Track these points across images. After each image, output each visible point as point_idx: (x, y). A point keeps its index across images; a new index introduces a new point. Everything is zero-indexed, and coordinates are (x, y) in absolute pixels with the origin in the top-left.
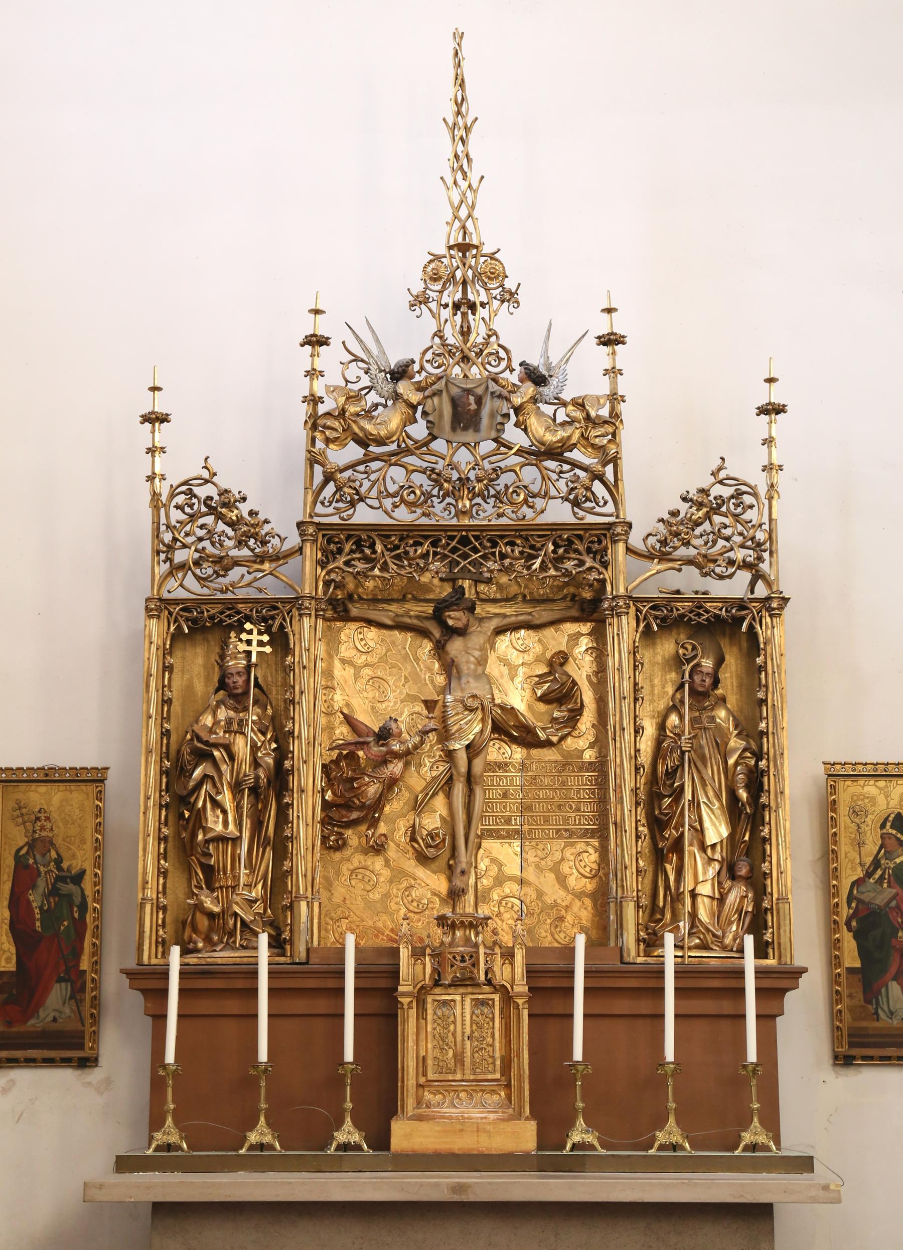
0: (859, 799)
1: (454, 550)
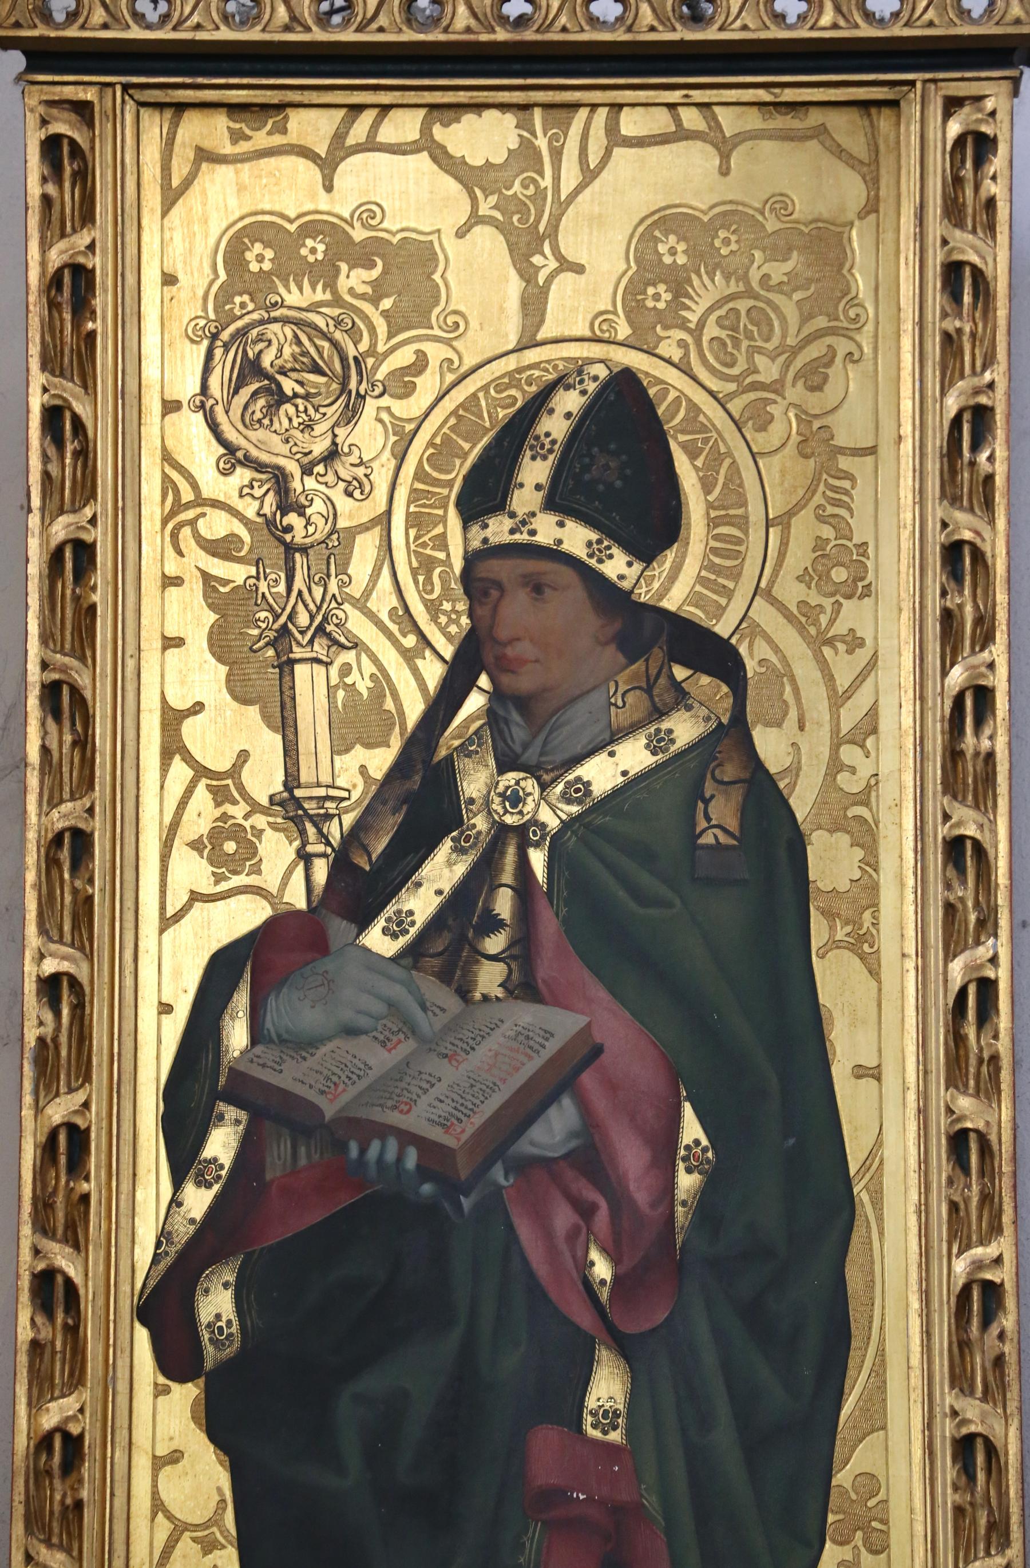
0: (290, 268)
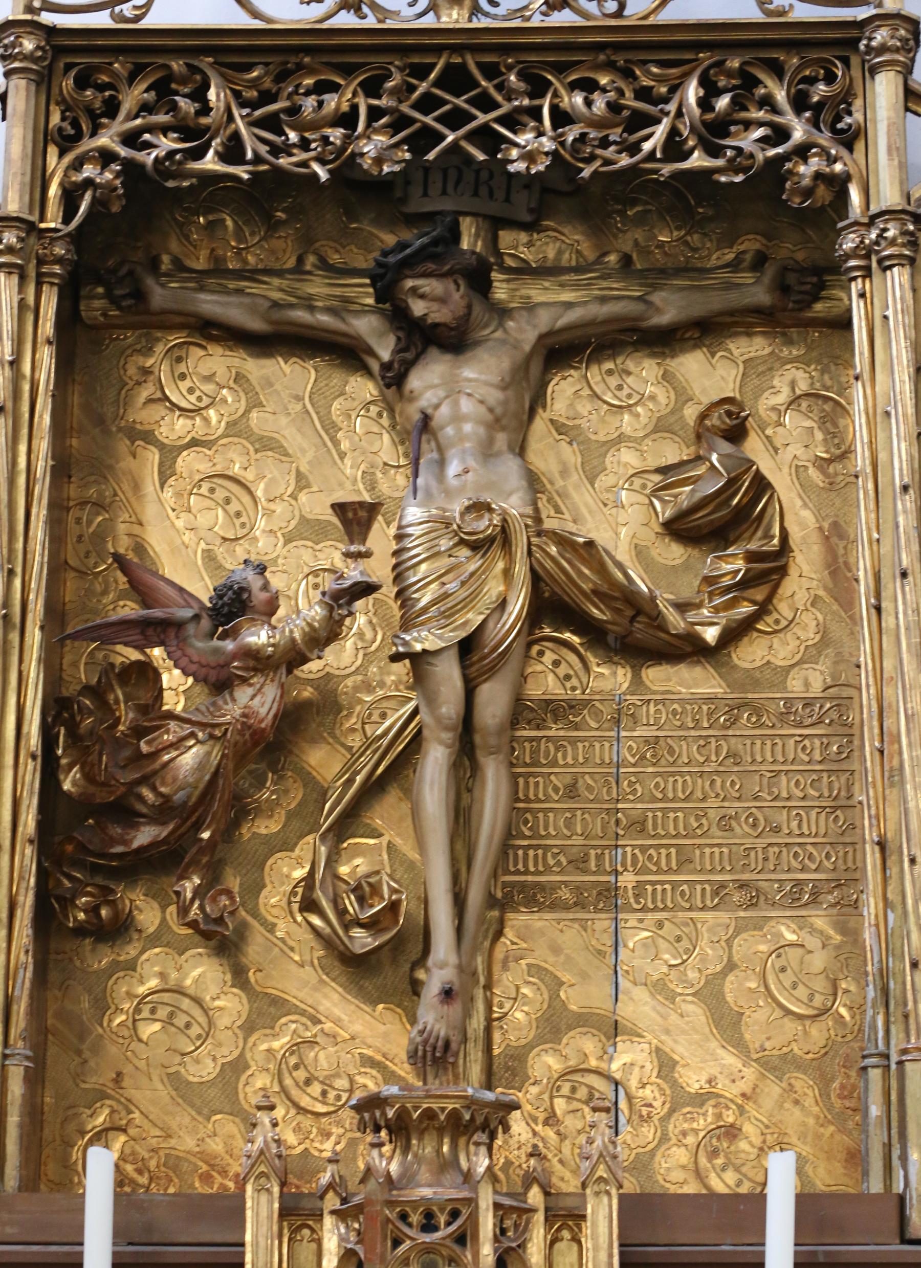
1: (427, 104)
